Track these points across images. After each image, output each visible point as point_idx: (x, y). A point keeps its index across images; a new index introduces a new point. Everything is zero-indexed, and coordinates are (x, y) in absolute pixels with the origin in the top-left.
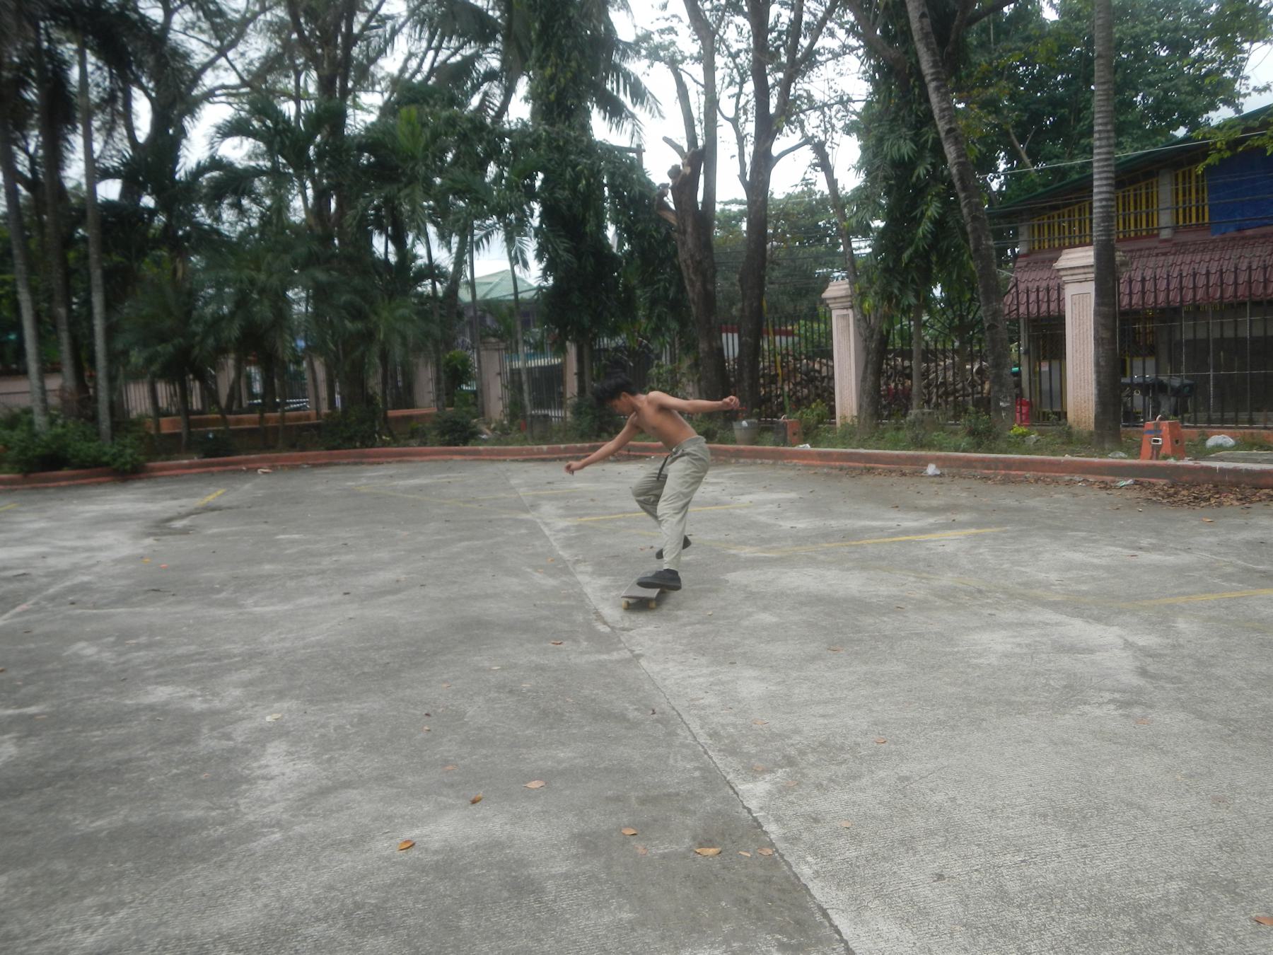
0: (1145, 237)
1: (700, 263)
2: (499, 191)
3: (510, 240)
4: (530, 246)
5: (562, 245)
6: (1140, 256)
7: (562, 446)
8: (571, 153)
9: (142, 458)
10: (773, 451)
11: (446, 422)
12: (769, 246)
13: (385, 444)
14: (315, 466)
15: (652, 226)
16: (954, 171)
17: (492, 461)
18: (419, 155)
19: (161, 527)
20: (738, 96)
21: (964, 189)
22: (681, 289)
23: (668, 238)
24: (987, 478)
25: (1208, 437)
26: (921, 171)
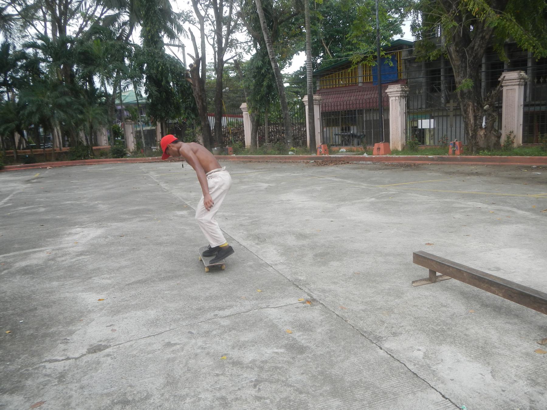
0: (355, 85)
1: (201, 96)
2: (131, 71)
3: (135, 88)
4: (143, 90)
5: (154, 89)
6: (350, 92)
7: (156, 157)
8: (155, 57)
9: (3, 164)
10: (224, 157)
11: (114, 150)
12: (224, 90)
13: (91, 159)
14: (67, 166)
15: (185, 83)
16: (274, 71)
17: (132, 163)
18: (101, 55)
19: (28, 181)
20: (214, 39)
21: (277, 76)
22: (195, 104)
23: (190, 88)
24: (280, 162)
25: (340, 149)
26: (263, 71)
